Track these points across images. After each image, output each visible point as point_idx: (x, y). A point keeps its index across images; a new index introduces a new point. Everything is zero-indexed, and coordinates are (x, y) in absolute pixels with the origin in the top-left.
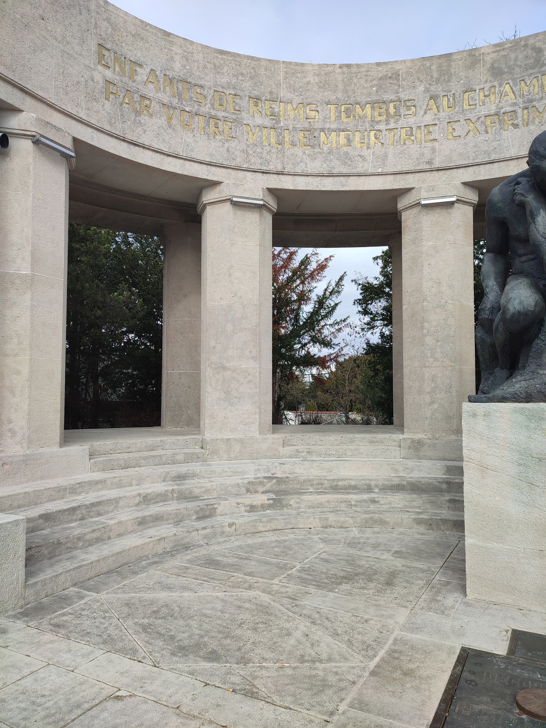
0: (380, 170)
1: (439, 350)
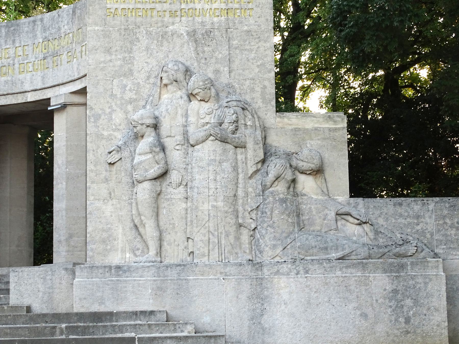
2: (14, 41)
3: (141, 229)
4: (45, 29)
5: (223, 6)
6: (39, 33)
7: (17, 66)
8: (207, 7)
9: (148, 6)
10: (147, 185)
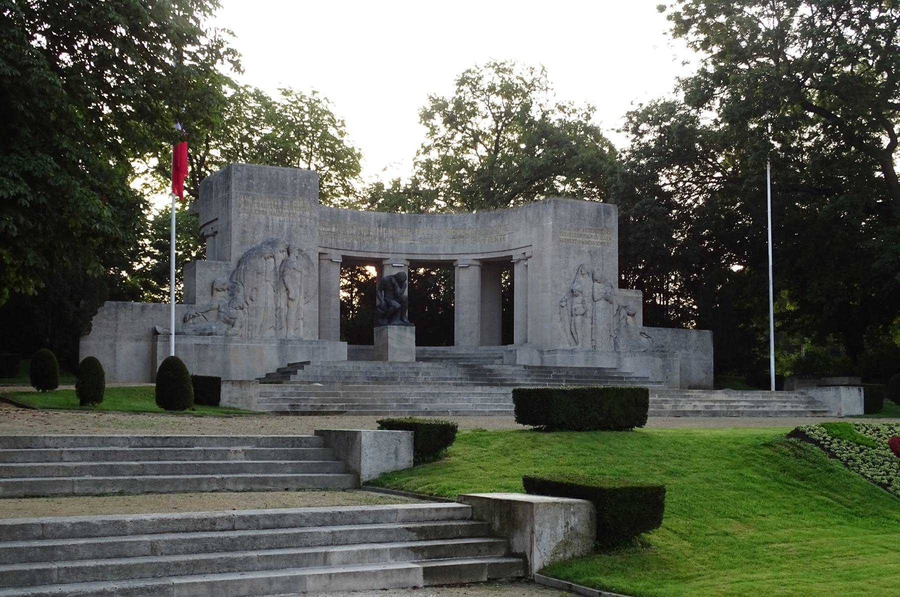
2: (432, 226)
3: (575, 335)
4: (453, 223)
5: (601, 241)
6: (449, 224)
7: (434, 239)
8: (595, 241)
9: (574, 238)
10: (580, 317)
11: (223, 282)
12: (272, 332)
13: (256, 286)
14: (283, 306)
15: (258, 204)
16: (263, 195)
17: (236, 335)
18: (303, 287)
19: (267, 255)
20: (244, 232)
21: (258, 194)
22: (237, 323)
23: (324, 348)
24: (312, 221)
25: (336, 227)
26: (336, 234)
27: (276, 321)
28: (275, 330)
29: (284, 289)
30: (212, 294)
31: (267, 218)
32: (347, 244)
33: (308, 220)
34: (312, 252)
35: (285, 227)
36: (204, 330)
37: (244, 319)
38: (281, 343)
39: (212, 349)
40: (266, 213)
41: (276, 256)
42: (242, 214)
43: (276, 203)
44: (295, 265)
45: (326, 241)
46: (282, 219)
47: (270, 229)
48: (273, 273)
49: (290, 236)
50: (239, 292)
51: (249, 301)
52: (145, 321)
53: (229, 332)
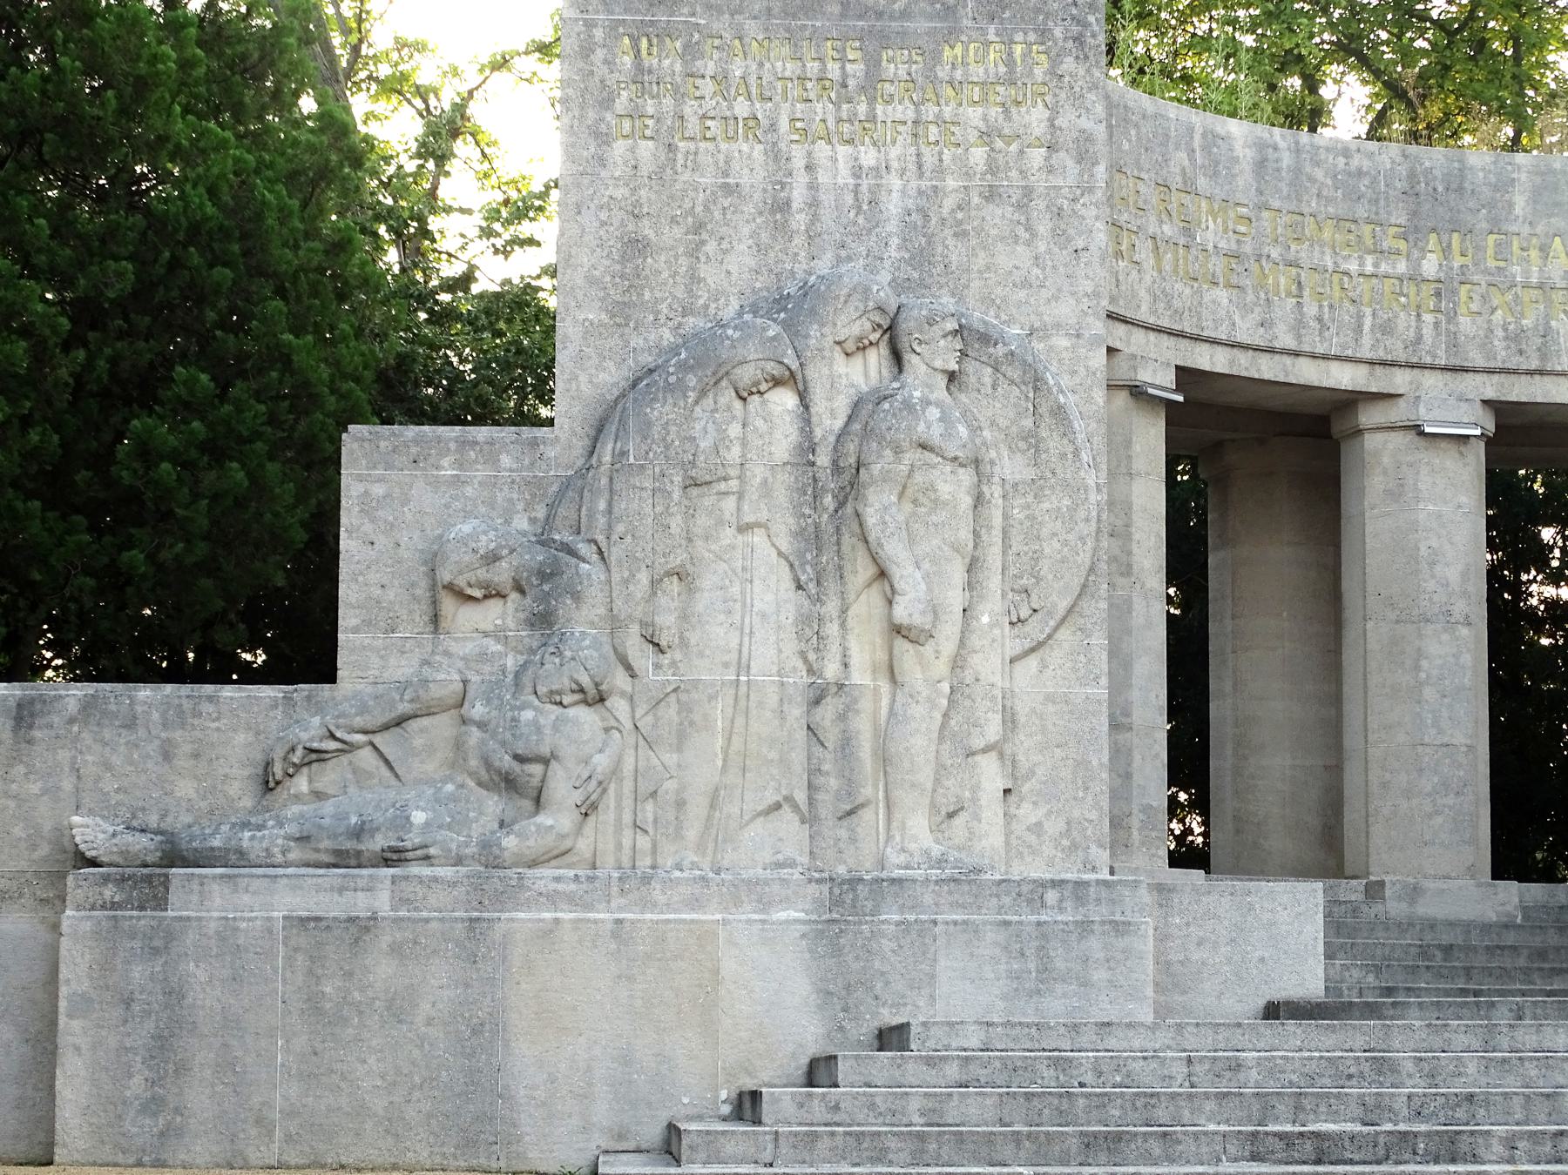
0: (1349, 353)
1: (1445, 713)
11: (486, 543)
12: (789, 833)
13: (675, 561)
14: (860, 676)
15: (721, 79)
16: (752, 28)
17: (558, 856)
18: (993, 557)
19: (746, 374)
20: (636, 247)
21: (722, 24)
22: (562, 787)
23: (1120, 928)
24: (1065, 159)
25: (1446, 251)
26: (1443, 289)
27: (814, 771)
28: (810, 818)
29: (871, 571)
30: (435, 619)
31: (776, 156)
32: (1516, 338)
33: (1037, 156)
34: (1062, 342)
35: (893, 205)
36: (358, 833)
37: (602, 762)
38: (836, 902)
39: (396, 949)
40: (773, 127)
41: (816, 375)
42: (620, 147)
43: (834, 69)
44: (930, 425)
45: (1386, 329)
46: (869, 157)
47: (799, 220)
48: (784, 480)
49: (921, 258)
50: (577, 597)
51: (642, 657)
52: (35, 788)
53: (510, 842)
